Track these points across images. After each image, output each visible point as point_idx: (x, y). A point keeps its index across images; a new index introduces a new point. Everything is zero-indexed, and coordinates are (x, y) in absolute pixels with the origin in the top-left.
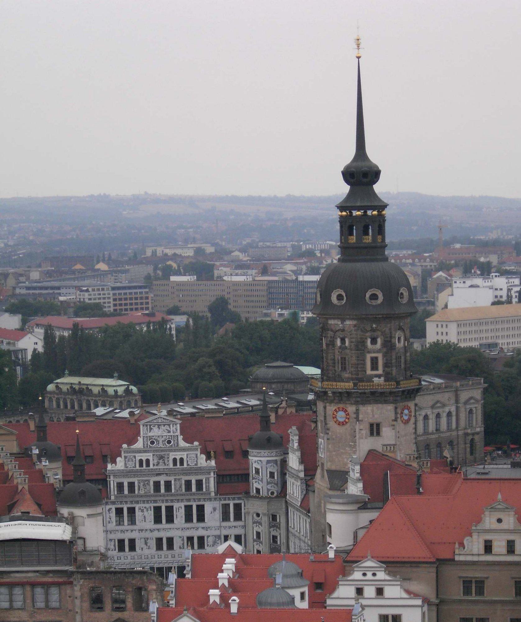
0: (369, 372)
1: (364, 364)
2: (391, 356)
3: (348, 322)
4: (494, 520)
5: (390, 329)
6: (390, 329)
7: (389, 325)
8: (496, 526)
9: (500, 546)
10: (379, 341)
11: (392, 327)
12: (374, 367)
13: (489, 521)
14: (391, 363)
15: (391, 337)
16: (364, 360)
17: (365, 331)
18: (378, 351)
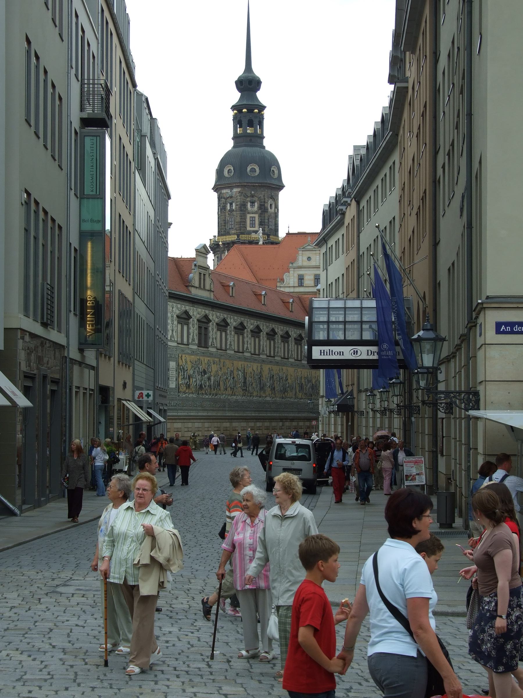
0: (249, 228)
1: (245, 222)
2: (264, 217)
3: (235, 190)
4: (305, 258)
5: (264, 196)
6: (264, 196)
7: (263, 193)
8: (306, 263)
9: (309, 280)
10: (256, 205)
11: (266, 195)
12: (253, 225)
13: (302, 259)
14: (264, 222)
15: (264, 202)
16: (245, 219)
17: (246, 196)
18: (255, 213)
